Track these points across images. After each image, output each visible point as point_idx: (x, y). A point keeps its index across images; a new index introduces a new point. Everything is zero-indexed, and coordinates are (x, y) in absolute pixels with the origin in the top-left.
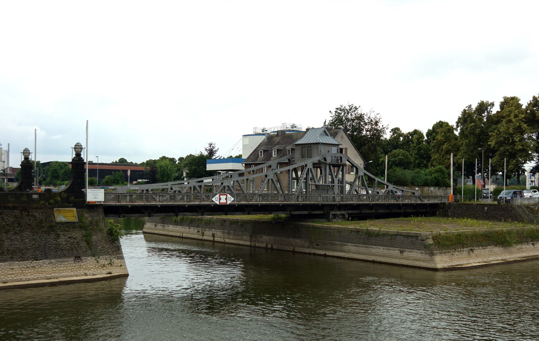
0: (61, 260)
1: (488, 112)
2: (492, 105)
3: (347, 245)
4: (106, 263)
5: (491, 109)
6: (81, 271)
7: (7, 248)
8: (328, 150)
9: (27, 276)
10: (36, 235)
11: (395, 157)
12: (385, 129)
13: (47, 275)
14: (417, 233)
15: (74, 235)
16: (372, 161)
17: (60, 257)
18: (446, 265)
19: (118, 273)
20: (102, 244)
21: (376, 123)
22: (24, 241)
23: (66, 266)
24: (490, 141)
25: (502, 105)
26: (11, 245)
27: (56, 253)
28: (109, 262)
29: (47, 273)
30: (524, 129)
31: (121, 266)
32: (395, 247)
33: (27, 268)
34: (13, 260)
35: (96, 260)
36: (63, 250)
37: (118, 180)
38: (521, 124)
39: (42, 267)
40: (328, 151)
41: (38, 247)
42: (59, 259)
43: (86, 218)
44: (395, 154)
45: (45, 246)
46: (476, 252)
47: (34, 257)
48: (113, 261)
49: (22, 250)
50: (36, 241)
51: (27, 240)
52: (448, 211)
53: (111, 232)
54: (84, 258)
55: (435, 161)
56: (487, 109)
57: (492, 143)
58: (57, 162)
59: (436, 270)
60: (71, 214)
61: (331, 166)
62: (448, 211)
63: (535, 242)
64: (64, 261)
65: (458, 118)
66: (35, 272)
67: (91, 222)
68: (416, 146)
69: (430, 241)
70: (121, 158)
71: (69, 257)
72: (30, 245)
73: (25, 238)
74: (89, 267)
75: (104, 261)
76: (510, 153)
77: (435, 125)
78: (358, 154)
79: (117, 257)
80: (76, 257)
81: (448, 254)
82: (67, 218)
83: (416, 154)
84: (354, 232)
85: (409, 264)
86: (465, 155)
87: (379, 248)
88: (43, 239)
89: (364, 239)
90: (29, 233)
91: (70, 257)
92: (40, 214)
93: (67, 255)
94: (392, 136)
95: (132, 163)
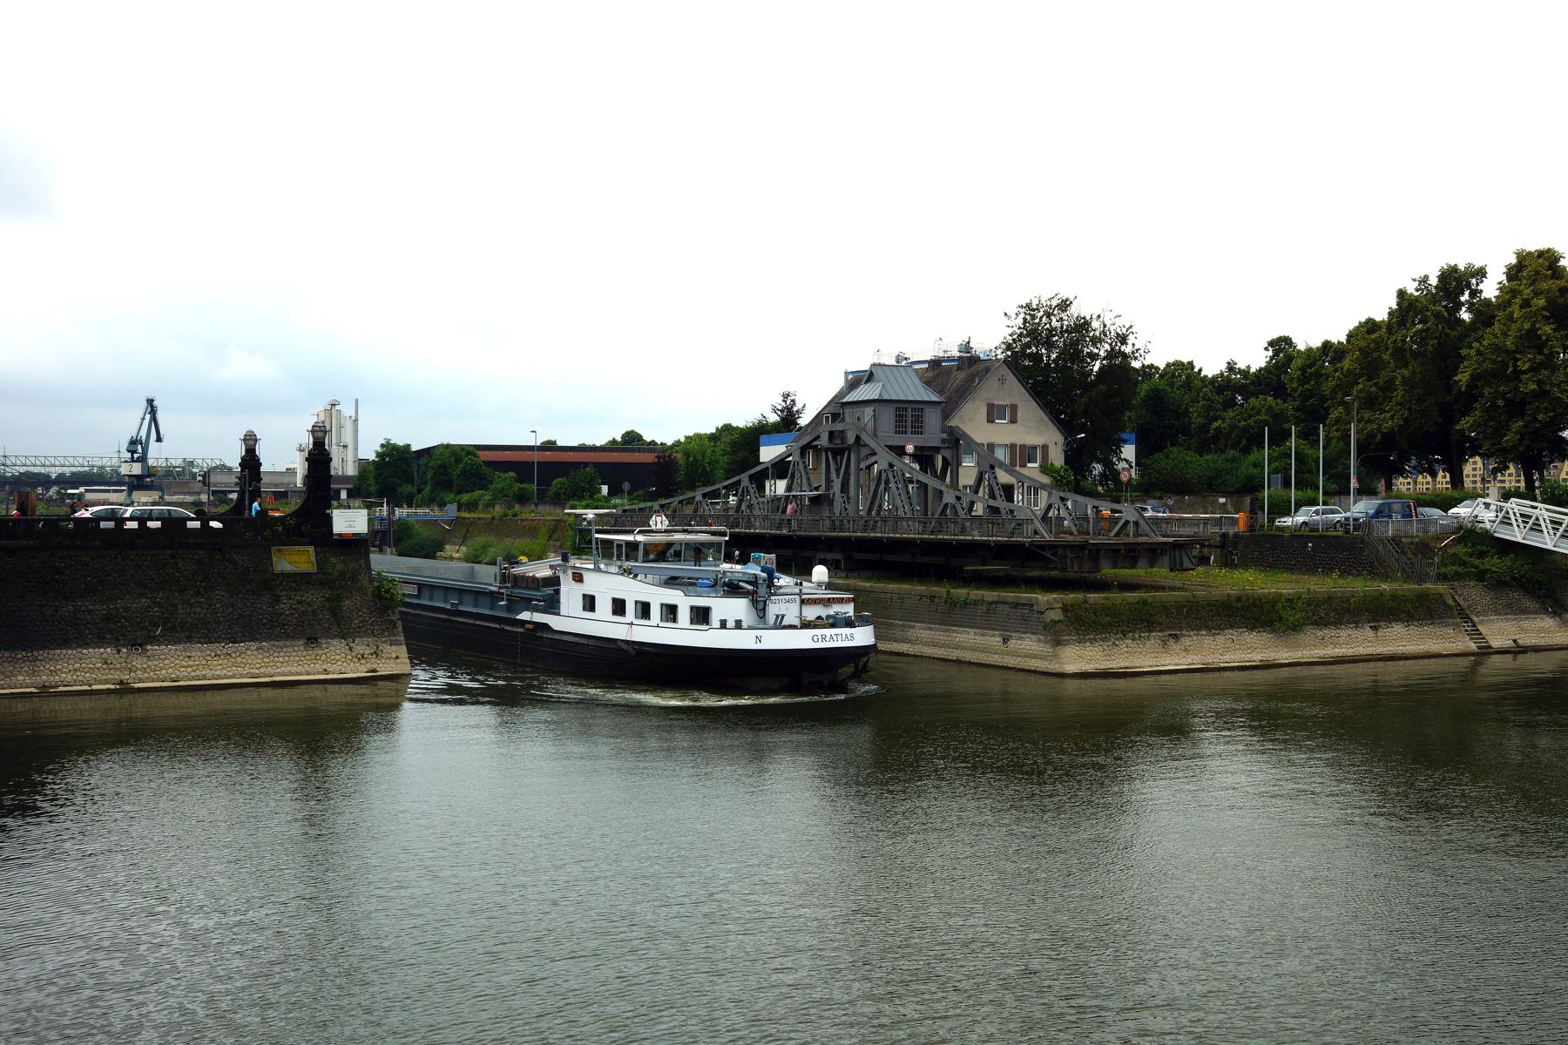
0: (280, 643)
1: (1474, 293)
2: (1481, 273)
3: (913, 627)
4: (368, 652)
5: (1478, 284)
6: (317, 665)
7: (182, 619)
10: (235, 597)
11: (1250, 416)
12: (1141, 352)
13: (252, 671)
14: (1032, 597)
15: (308, 597)
16: (1083, 435)
17: (278, 638)
18: (1089, 667)
21: (1123, 339)
25: (1514, 273)
28: (373, 651)
31: (397, 657)
32: (995, 630)
33: (216, 656)
35: (347, 645)
36: (284, 625)
37: (584, 489)
38: (1537, 326)
39: (243, 656)
40: (859, 419)
41: (238, 619)
42: (277, 641)
43: (334, 566)
44: (1253, 409)
46: (1186, 641)
47: (229, 636)
48: (381, 648)
49: (209, 622)
51: (218, 606)
53: (381, 592)
54: (323, 641)
55: (1334, 428)
56: (1469, 285)
57: (1463, 378)
58: (448, 446)
59: (1062, 675)
60: (303, 558)
61: (829, 453)
62: (1233, 554)
63: (1382, 624)
64: (287, 647)
65: (1389, 313)
66: (230, 664)
67: (342, 573)
68: (1298, 387)
69: (1056, 615)
70: (629, 429)
73: (215, 602)
74: (333, 657)
75: (363, 647)
76: (1509, 403)
77: (1356, 329)
79: (391, 640)
80: (308, 639)
81: (1101, 643)
83: (1296, 409)
84: (926, 597)
85: (1018, 667)
86: (1401, 409)
87: (968, 633)
88: (248, 605)
89: (943, 613)
90: (222, 594)
94: (1272, 358)
95: (653, 442)
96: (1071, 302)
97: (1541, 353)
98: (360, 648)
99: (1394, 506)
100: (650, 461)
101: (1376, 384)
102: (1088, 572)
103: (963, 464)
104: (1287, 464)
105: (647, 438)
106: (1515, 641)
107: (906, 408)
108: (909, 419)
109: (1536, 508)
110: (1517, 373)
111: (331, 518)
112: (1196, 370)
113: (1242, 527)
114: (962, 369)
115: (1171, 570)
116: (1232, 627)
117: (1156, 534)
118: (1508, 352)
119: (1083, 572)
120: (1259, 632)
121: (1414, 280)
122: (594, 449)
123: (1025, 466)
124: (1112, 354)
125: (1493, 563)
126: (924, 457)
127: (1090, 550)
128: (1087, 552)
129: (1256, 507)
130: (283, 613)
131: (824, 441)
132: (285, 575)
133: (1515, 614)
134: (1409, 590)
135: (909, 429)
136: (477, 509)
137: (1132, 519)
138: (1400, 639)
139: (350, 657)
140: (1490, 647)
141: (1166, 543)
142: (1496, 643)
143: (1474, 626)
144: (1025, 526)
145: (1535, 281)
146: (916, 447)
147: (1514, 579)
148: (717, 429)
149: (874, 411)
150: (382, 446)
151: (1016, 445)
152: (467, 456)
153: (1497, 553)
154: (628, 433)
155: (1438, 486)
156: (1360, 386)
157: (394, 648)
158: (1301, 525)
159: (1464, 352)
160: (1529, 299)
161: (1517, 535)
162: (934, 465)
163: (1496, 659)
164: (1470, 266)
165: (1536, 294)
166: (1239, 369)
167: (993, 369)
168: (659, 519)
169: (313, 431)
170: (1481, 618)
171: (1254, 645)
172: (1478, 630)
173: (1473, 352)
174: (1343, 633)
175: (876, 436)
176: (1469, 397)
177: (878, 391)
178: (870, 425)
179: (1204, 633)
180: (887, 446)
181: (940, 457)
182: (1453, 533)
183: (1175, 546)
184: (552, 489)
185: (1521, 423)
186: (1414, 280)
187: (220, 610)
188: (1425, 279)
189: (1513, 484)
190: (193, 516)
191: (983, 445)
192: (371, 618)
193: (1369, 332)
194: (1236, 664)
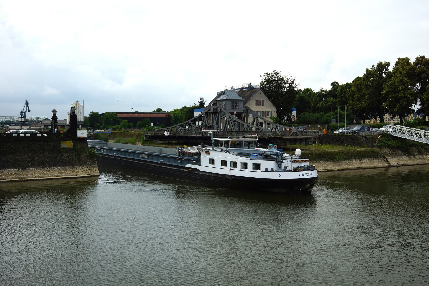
0: (63, 167)
1: (387, 70)
2: (388, 64)
4: (87, 169)
5: (387, 67)
8: (221, 104)
9: (46, 175)
11: (327, 103)
12: (297, 86)
15: (71, 155)
16: (282, 109)
17: (63, 166)
19: (94, 174)
20: (85, 160)
21: (292, 82)
22: (45, 157)
23: (66, 170)
24: (383, 91)
25: (397, 64)
26: (38, 159)
27: (61, 164)
28: (89, 169)
29: (56, 173)
30: (405, 82)
31: (96, 171)
34: (39, 167)
37: (146, 124)
38: (403, 78)
39: (53, 171)
44: (327, 101)
45: (55, 160)
48: (91, 168)
50: (51, 158)
51: (46, 157)
52: (322, 141)
53: (91, 153)
54: (75, 166)
55: (349, 106)
56: (385, 68)
57: (383, 93)
58: (109, 113)
62: (322, 141)
64: (65, 168)
65: (364, 75)
71: (67, 166)
72: (48, 159)
74: (78, 171)
75: (86, 168)
77: (355, 79)
78: (272, 104)
80: (71, 166)
82: (68, 146)
83: (339, 101)
86: (367, 101)
88: (54, 157)
90: (48, 154)
91: (68, 166)
92: (54, 144)
93: (66, 165)
94: (332, 87)
95: (165, 111)
96: (279, 73)
97: (404, 86)
98: (86, 168)
99: (365, 127)
100: (164, 117)
101: (360, 94)
102: (283, 146)
103: (249, 117)
104: (337, 116)
105: (163, 110)
106: (397, 163)
107: (234, 102)
108: (235, 105)
109: (403, 127)
110: (398, 91)
111: (77, 133)
112: (312, 91)
113: (325, 133)
114: (249, 91)
115: (306, 145)
116: (322, 160)
117: (301, 135)
118: (396, 86)
119: (282, 146)
120: (329, 161)
121: (371, 66)
122: (149, 113)
123: (266, 117)
124: (290, 87)
125: (391, 142)
126: (239, 115)
127: (284, 140)
128: (283, 140)
129: (328, 128)
130: (64, 159)
131: (211, 111)
132: (64, 148)
133: (398, 156)
134: (369, 150)
135: (235, 107)
136: (117, 130)
137: (295, 131)
138: (367, 163)
139: (82, 171)
140: (391, 165)
141: (304, 138)
142: (392, 164)
143: (387, 159)
144: (266, 133)
145: (403, 66)
146: (236, 112)
147: (397, 147)
148: (182, 108)
149: (225, 102)
150: (91, 113)
151: (264, 111)
152: (114, 115)
153: (393, 140)
154: (158, 109)
155: (377, 122)
156: (356, 95)
157: (95, 168)
158: (340, 133)
159: (384, 86)
160: (401, 71)
161: (398, 135)
162: (241, 117)
163: (392, 168)
164: (385, 62)
165: (403, 70)
166: (324, 90)
167: (257, 91)
168: (167, 132)
169: (72, 109)
170: (388, 157)
171: (328, 165)
172: (387, 161)
173: (386, 86)
174: (352, 162)
175: (226, 109)
176: (385, 98)
177: (226, 97)
178: (224, 106)
179: (315, 162)
180: (229, 112)
181: (243, 115)
182: (381, 134)
183: (307, 138)
184: (137, 125)
185: (399, 105)
186: (371, 66)
187: (47, 158)
188: (373, 66)
189: (397, 121)
190: (39, 133)
191: (255, 111)
192: (88, 160)
193: (359, 80)
194: (323, 170)
